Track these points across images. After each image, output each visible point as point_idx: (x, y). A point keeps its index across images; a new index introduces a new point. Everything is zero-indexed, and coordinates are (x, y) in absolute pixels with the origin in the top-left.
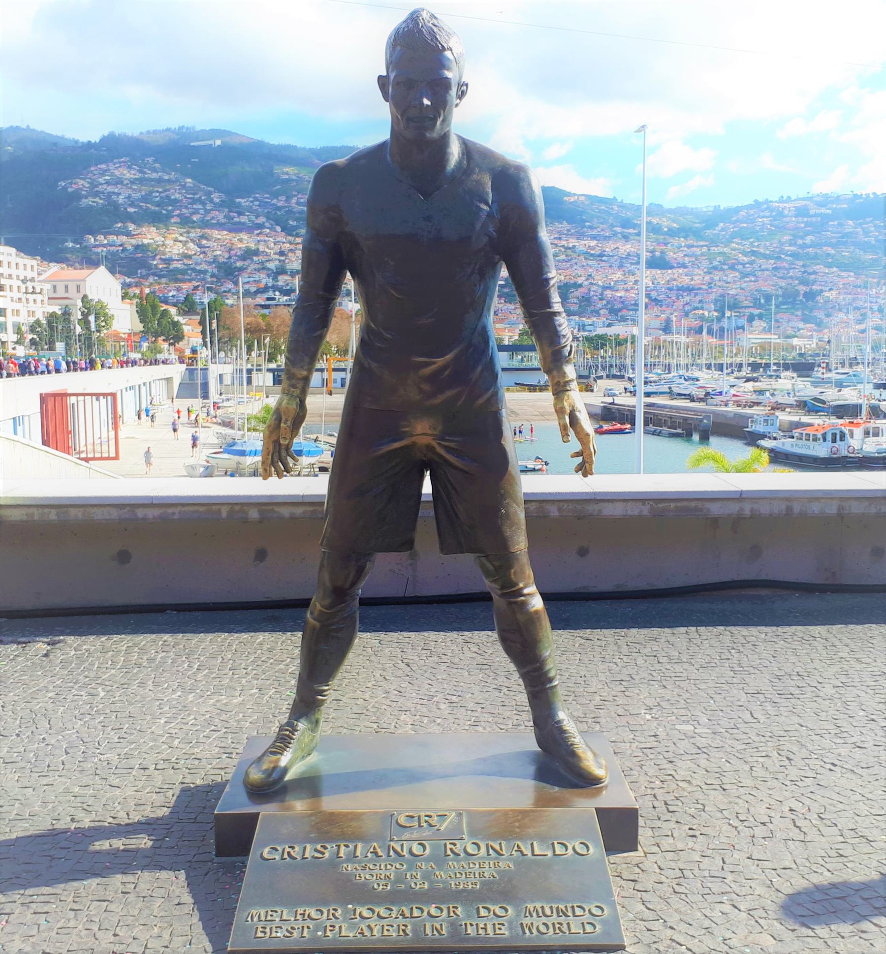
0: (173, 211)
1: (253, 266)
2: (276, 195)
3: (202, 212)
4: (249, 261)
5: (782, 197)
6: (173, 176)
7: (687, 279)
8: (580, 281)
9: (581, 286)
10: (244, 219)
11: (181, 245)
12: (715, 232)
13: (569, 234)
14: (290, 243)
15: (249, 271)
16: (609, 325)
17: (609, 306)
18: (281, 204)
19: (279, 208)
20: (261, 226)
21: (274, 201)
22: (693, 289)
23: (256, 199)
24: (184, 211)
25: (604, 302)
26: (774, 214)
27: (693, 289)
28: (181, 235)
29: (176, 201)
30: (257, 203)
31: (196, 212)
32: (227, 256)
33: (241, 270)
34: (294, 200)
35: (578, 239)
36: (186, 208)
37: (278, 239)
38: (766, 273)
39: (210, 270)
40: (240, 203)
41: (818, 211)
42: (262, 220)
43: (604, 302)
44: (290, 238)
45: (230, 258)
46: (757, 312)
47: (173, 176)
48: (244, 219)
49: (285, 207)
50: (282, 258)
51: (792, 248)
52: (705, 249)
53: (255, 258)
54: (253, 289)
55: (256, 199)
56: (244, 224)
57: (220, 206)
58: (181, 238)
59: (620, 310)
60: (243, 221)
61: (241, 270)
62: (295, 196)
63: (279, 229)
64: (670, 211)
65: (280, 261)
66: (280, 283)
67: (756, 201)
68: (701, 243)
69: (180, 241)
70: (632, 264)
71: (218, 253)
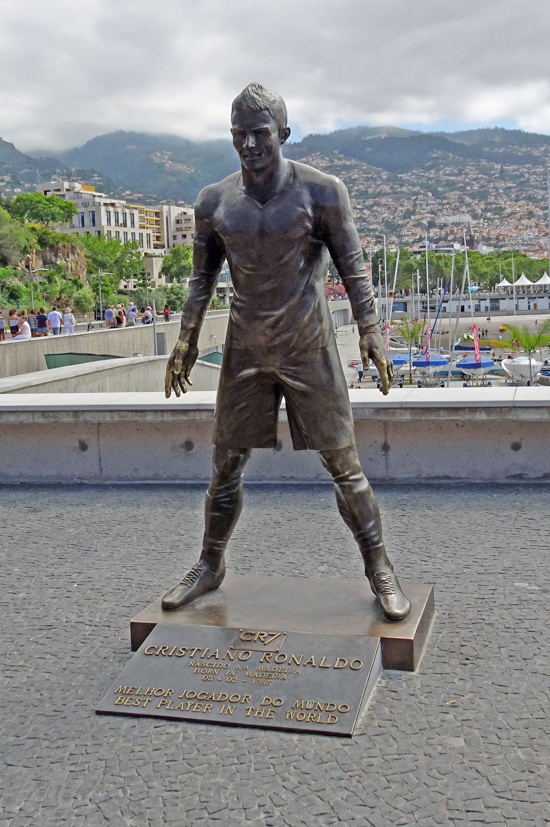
0: (352, 187)
1: (411, 224)
2: (429, 169)
3: (374, 186)
4: (408, 220)
6: (353, 162)
10: (404, 189)
11: (358, 211)
14: (439, 204)
15: (408, 226)
18: (432, 176)
19: (430, 179)
20: (416, 194)
21: (427, 174)
23: (414, 174)
24: (361, 187)
28: (359, 204)
29: (355, 180)
30: (414, 176)
31: (370, 187)
32: (392, 217)
33: (401, 226)
34: (441, 172)
36: (363, 184)
37: (430, 202)
39: (379, 228)
40: (401, 177)
42: (417, 189)
44: (439, 201)
45: (394, 218)
47: (353, 162)
48: (404, 189)
49: (434, 178)
50: (433, 216)
53: (413, 217)
54: (411, 241)
55: (414, 174)
56: (404, 192)
57: (387, 181)
58: (359, 207)
60: (404, 190)
61: (401, 226)
62: (443, 168)
63: (430, 194)
65: (431, 218)
66: (431, 235)
69: (358, 209)
71: (386, 215)
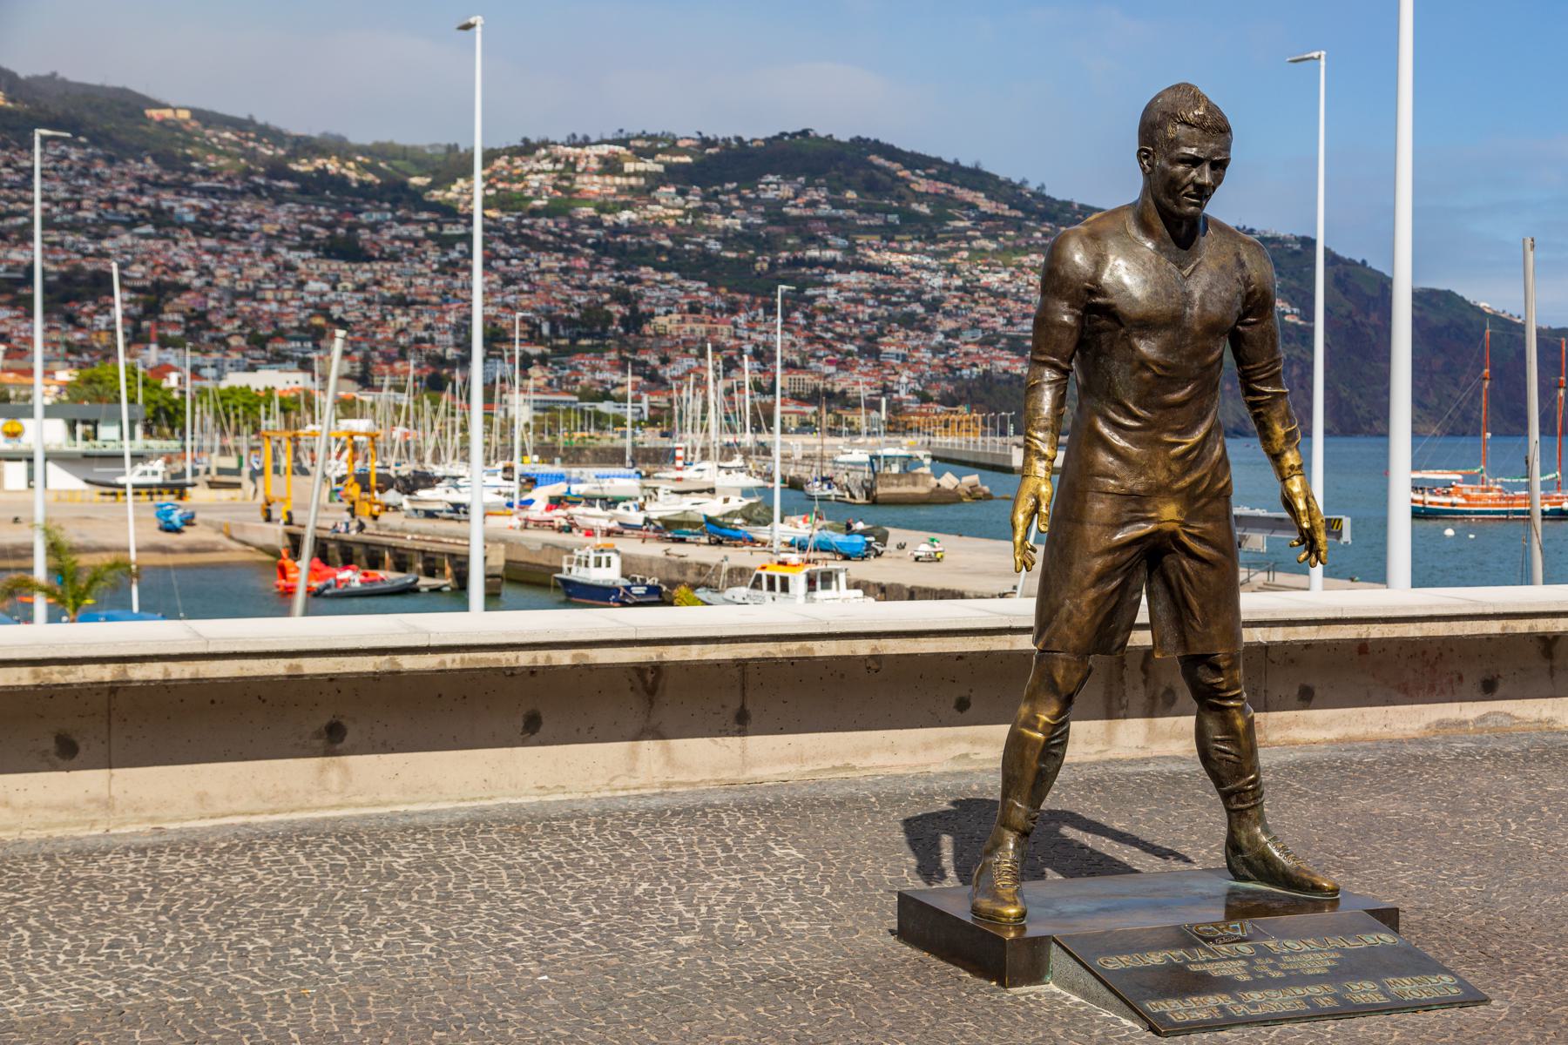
5: (574, 136)
7: (399, 283)
8: (186, 277)
9: (186, 288)
12: (449, 195)
13: (157, 184)
16: (252, 368)
17: (247, 330)
22: (414, 303)
25: (237, 323)
26: (559, 166)
27: (414, 303)
35: (178, 193)
38: (549, 278)
41: (641, 167)
43: (237, 323)
46: (534, 350)
51: (594, 232)
52: (432, 228)
59: (268, 339)
64: (363, 150)
67: (525, 141)
68: (425, 215)
70: (290, 248)
